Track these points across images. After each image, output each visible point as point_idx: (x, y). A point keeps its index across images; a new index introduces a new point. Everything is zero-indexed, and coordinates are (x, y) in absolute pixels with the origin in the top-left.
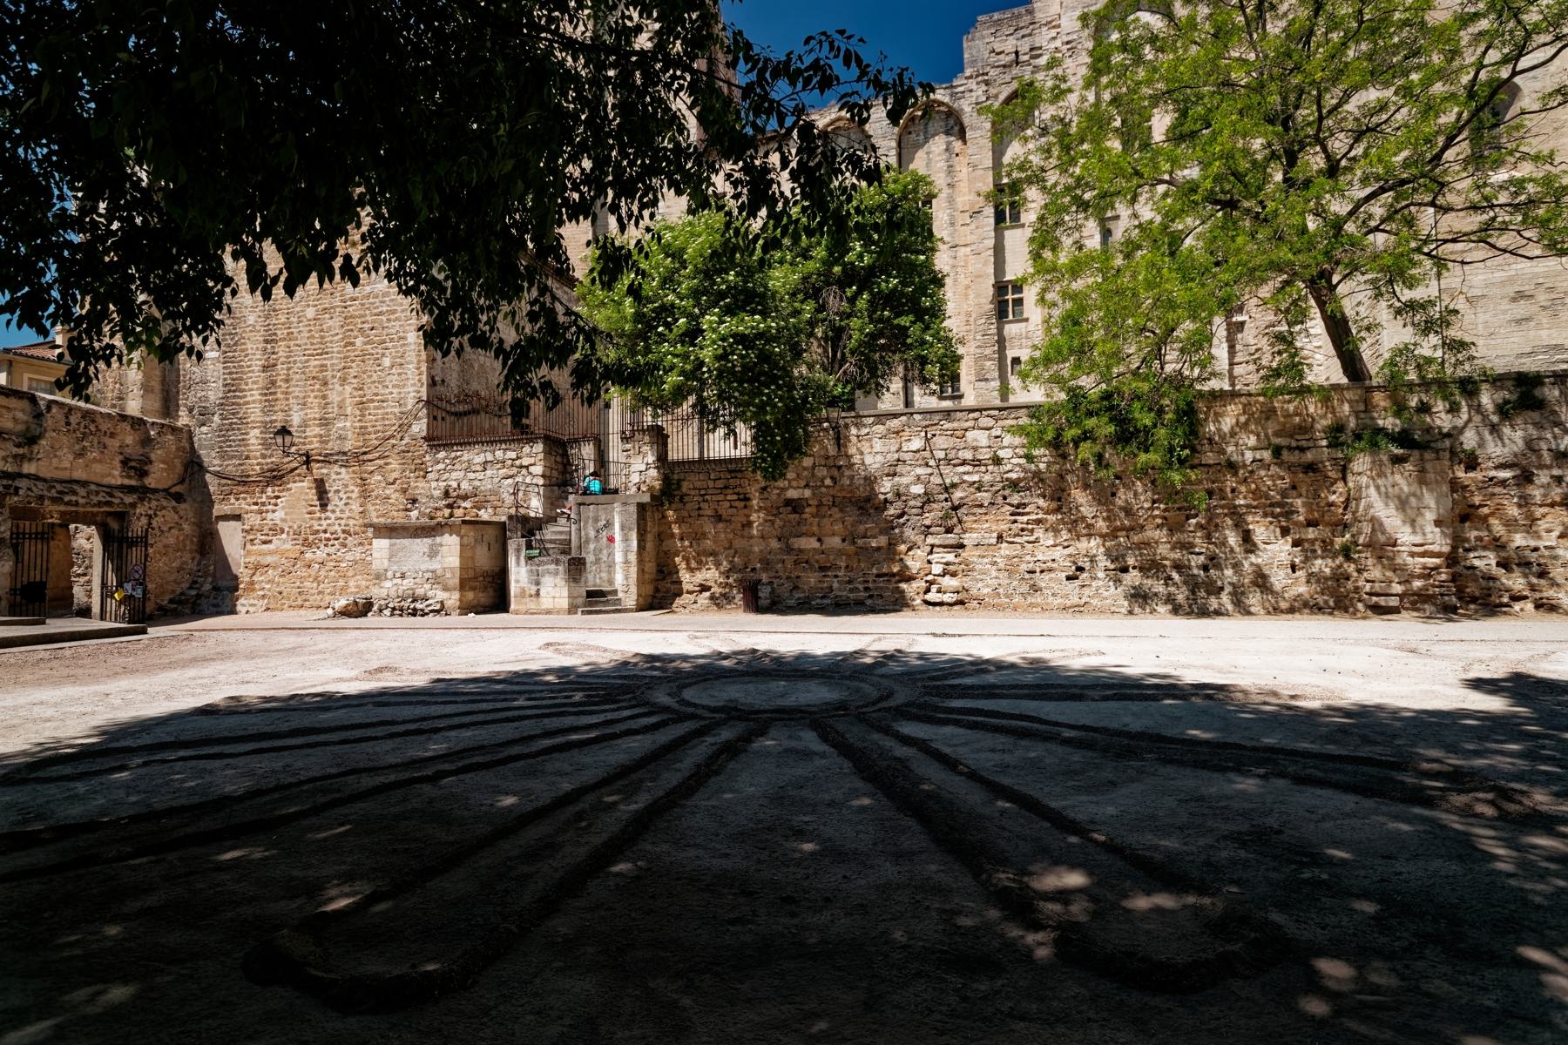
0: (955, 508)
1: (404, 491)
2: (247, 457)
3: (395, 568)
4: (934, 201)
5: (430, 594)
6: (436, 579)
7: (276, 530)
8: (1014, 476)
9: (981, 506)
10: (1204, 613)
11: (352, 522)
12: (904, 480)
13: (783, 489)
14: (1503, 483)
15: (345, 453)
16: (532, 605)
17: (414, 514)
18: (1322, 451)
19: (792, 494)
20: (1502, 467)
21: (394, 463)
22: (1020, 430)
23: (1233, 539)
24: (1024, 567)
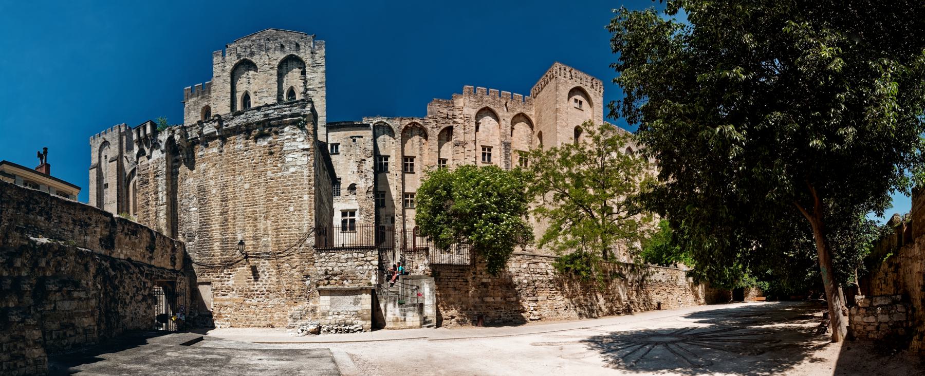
1: (302, 272)
7: (230, 290)
17: (308, 282)
21: (296, 258)
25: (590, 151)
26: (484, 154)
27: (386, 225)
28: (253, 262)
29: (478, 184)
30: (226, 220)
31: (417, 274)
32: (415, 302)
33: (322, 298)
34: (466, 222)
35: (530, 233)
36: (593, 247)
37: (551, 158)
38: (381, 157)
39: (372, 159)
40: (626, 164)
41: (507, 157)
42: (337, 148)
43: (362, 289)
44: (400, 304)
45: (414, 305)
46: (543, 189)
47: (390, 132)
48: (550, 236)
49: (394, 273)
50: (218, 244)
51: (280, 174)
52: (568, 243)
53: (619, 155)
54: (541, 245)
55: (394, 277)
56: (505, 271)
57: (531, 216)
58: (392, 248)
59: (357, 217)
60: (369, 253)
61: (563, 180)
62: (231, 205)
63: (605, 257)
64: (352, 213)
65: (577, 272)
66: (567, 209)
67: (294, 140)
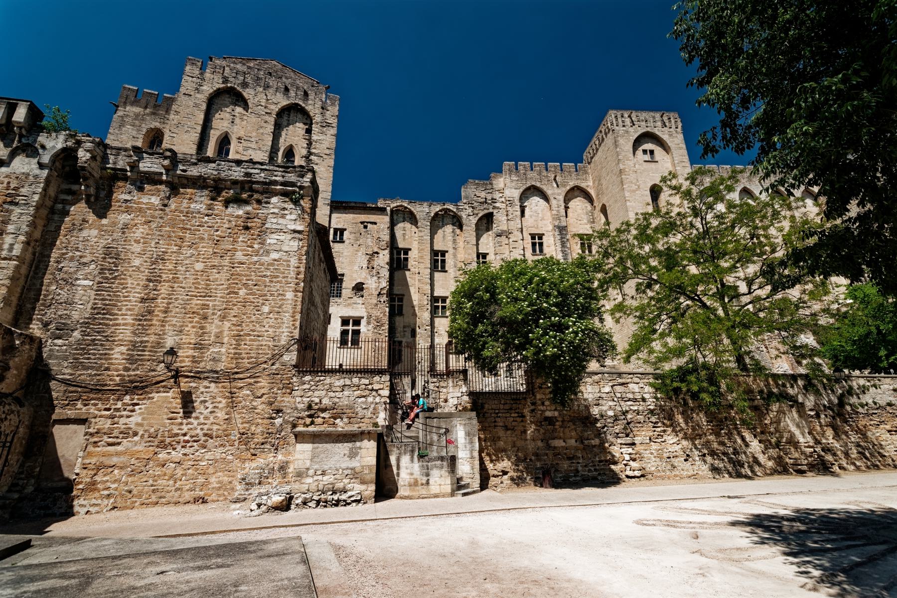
0: (628, 423)
1: (271, 404)
2: (107, 369)
3: (316, 467)
4: (447, 254)
5: (349, 486)
6: (355, 475)
7: (127, 433)
8: (652, 407)
9: (640, 423)
10: (739, 476)
11: (215, 427)
12: (604, 408)
13: (543, 411)
14: (812, 417)
15: (216, 372)
16: (423, 491)
17: (278, 421)
18: (759, 401)
19: (548, 414)
20: (811, 410)
21: (264, 382)
22: (651, 385)
23: (739, 441)
24: (665, 455)
25: (679, 214)
26: (534, 244)
27: (404, 340)
28: (185, 384)
29: (530, 282)
30: (150, 312)
31: (446, 410)
32: (444, 454)
33: (300, 447)
34: (517, 332)
35: (609, 341)
36: (716, 352)
37: (623, 237)
38: (399, 250)
39: (387, 252)
40: (746, 215)
41: (563, 245)
42: (342, 235)
43: (362, 433)
44: (421, 457)
45: (442, 459)
46: (619, 280)
47: (412, 219)
48: (639, 343)
49: (412, 409)
50: (124, 349)
51: (256, 259)
52: (670, 351)
53: (731, 206)
54: (629, 357)
55: (412, 415)
56: (577, 399)
57: (607, 318)
58: (411, 372)
59: (363, 328)
60: (377, 378)
61: (646, 263)
62: (164, 289)
63: (743, 367)
64: (357, 322)
65: (695, 396)
66: (659, 300)
67: (283, 216)
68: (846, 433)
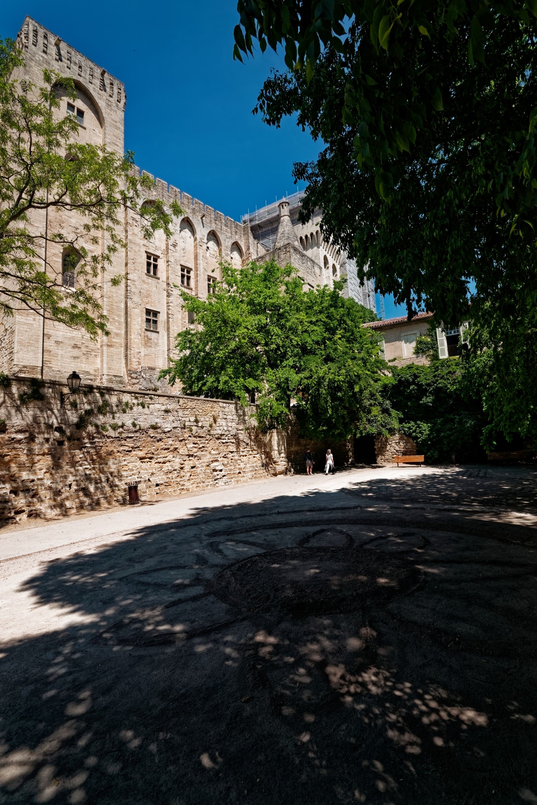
14: (19, 441)
68: (73, 464)
